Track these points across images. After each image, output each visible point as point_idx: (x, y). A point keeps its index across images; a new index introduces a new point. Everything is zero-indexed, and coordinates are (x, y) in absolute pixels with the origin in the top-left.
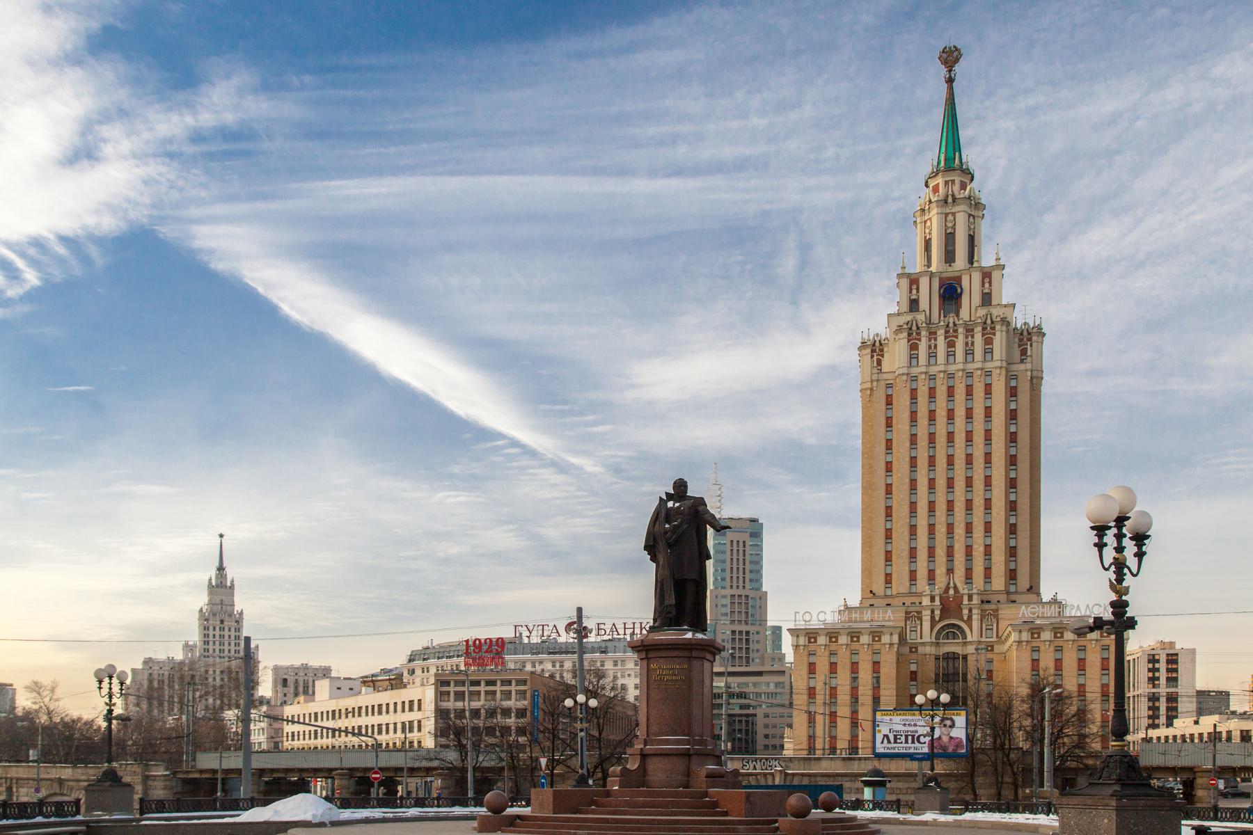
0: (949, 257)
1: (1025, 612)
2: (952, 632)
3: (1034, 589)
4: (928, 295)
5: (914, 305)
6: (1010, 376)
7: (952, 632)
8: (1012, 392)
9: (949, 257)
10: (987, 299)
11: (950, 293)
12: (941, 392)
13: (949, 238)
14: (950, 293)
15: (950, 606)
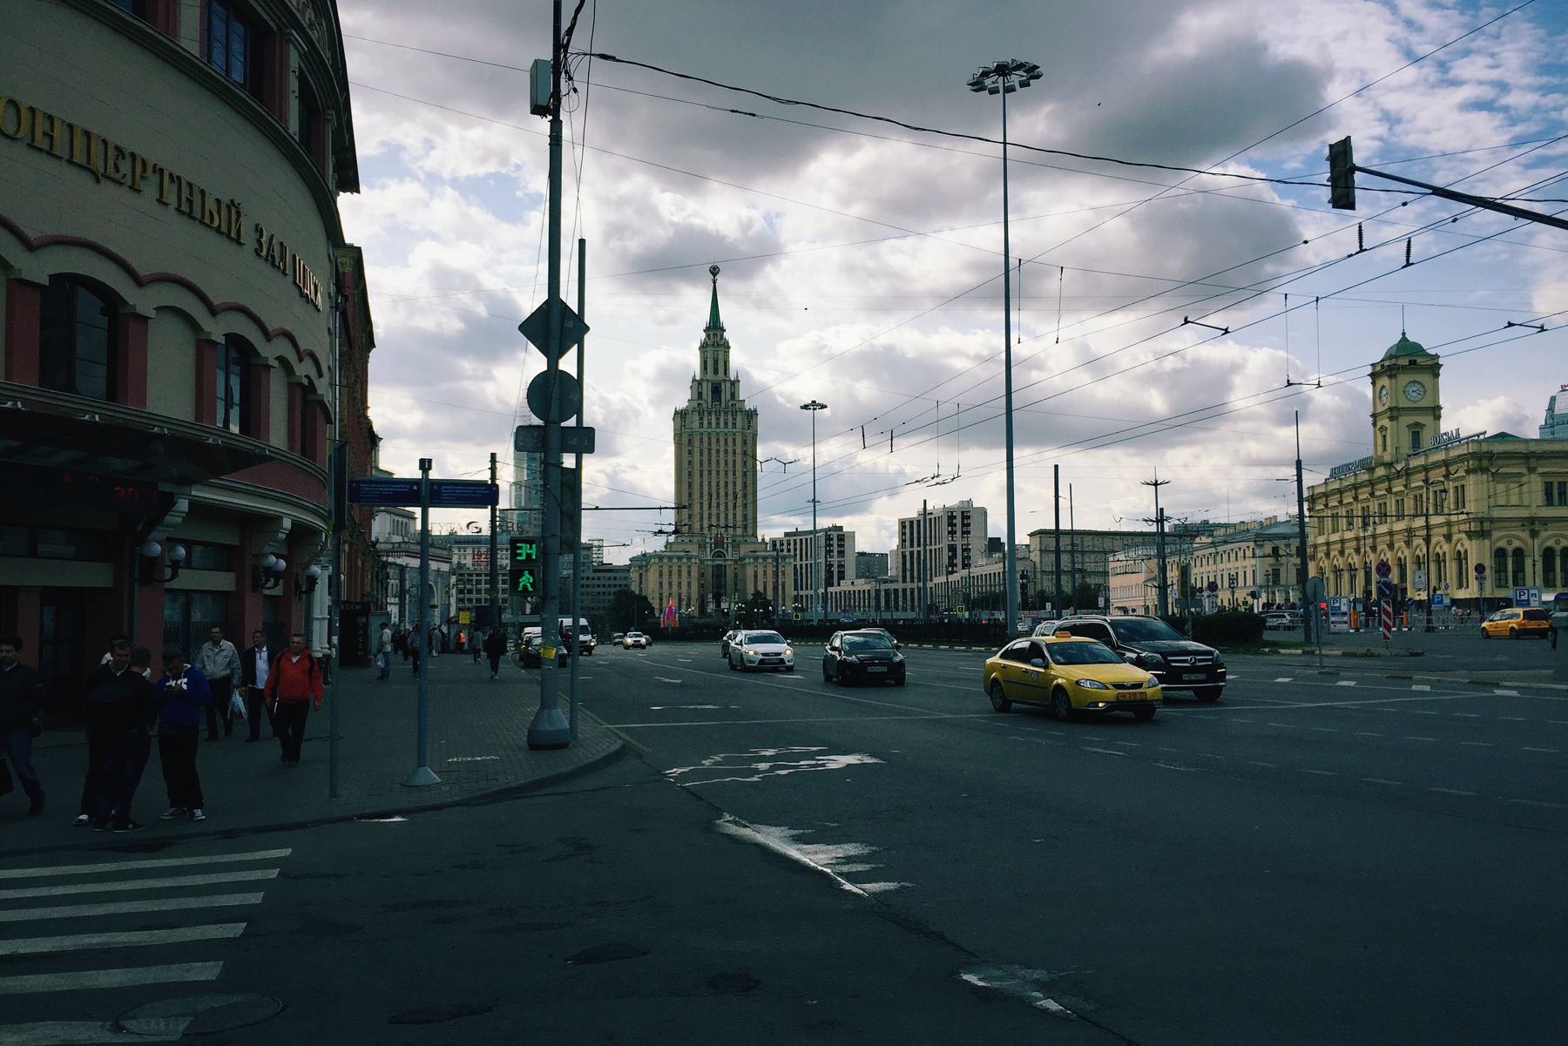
0: (716, 371)
1: (752, 548)
2: (720, 555)
3: (755, 535)
4: (707, 390)
5: (700, 394)
6: (744, 435)
7: (720, 555)
8: (745, 443)
9: (716, 371)
10: (733, 395)
11: (716, 390)
12: (714, 440)
13: (716, 362)
14: (716, 390)
15: (719, 543)
